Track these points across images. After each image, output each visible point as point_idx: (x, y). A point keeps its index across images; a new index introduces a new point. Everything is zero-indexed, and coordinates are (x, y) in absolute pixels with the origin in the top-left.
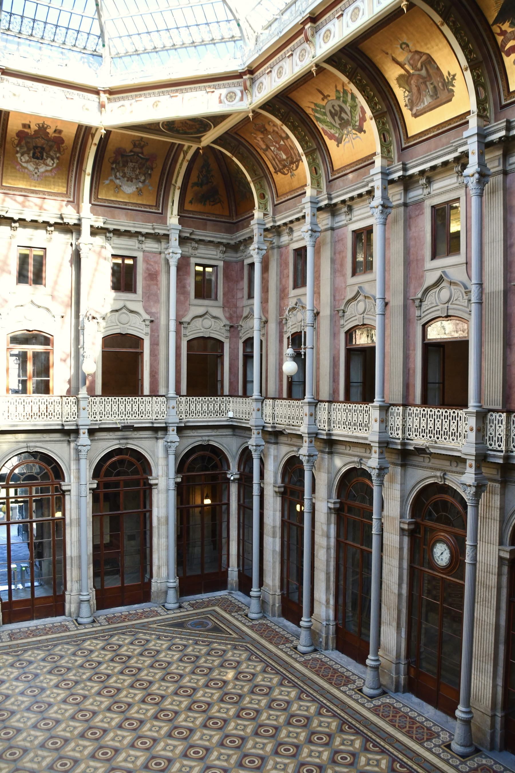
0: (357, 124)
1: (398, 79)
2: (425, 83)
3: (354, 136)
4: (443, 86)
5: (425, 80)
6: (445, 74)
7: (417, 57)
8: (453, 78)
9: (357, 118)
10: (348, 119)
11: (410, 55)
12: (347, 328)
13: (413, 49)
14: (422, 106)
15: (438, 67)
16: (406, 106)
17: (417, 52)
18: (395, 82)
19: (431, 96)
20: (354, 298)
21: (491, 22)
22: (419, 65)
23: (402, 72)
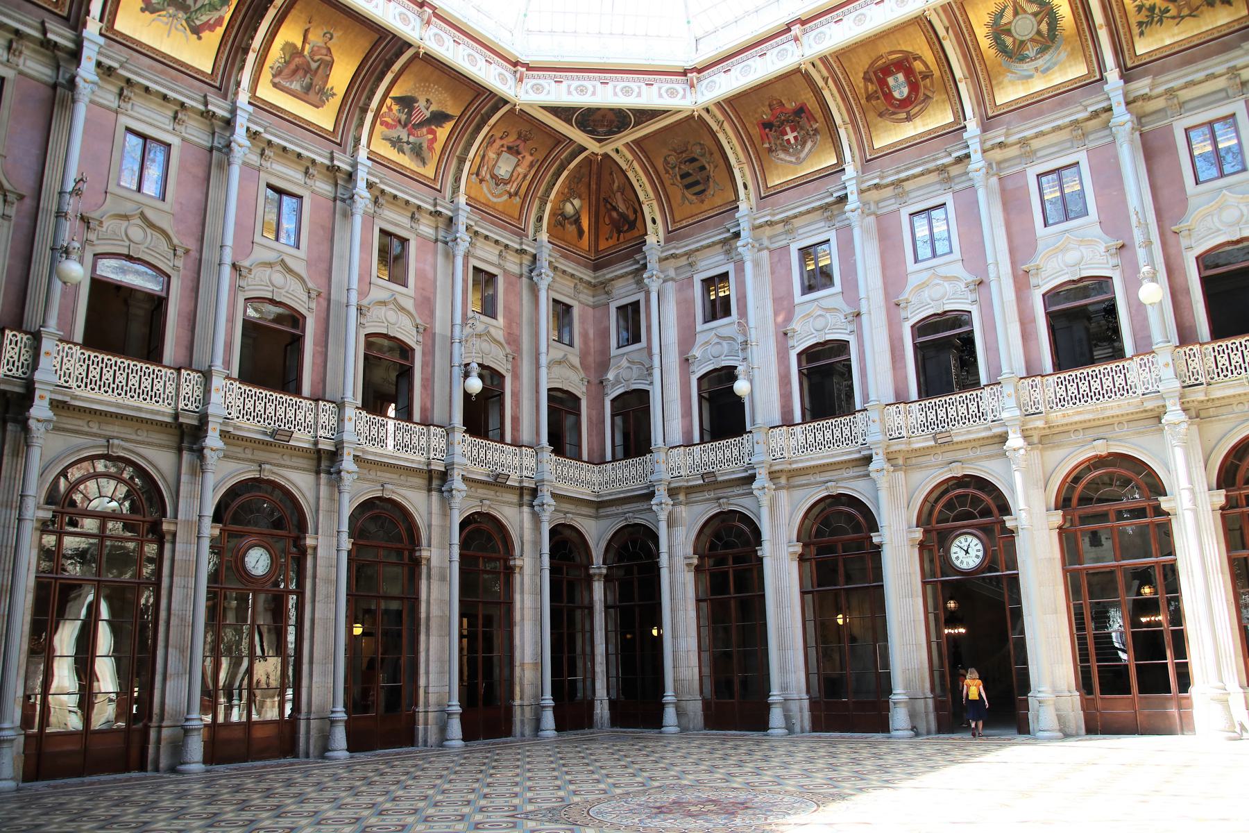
0: (198, 23)
1: (287, 44)
2: (306, 73)
3: (180, 27)
4: (319, 91)
5: (307, 70)
6: (329, 86)
7: (324, 51)
8: (333, 95)
9: (204, 18)
10: (189, 7)
11: (321, 44)
12: (100, 250)
13: (330, 44)
14: (288, 85)
15: (328, 76)
16: (272, 68)
17: (329, 50)
18: (283, 42)
19: (302, 87)
20: (126, 217)
21: (391, 95)
22: (317, 58)
23: (299, 45)
